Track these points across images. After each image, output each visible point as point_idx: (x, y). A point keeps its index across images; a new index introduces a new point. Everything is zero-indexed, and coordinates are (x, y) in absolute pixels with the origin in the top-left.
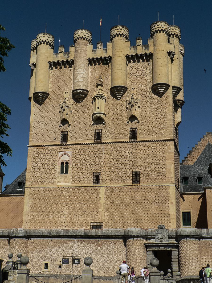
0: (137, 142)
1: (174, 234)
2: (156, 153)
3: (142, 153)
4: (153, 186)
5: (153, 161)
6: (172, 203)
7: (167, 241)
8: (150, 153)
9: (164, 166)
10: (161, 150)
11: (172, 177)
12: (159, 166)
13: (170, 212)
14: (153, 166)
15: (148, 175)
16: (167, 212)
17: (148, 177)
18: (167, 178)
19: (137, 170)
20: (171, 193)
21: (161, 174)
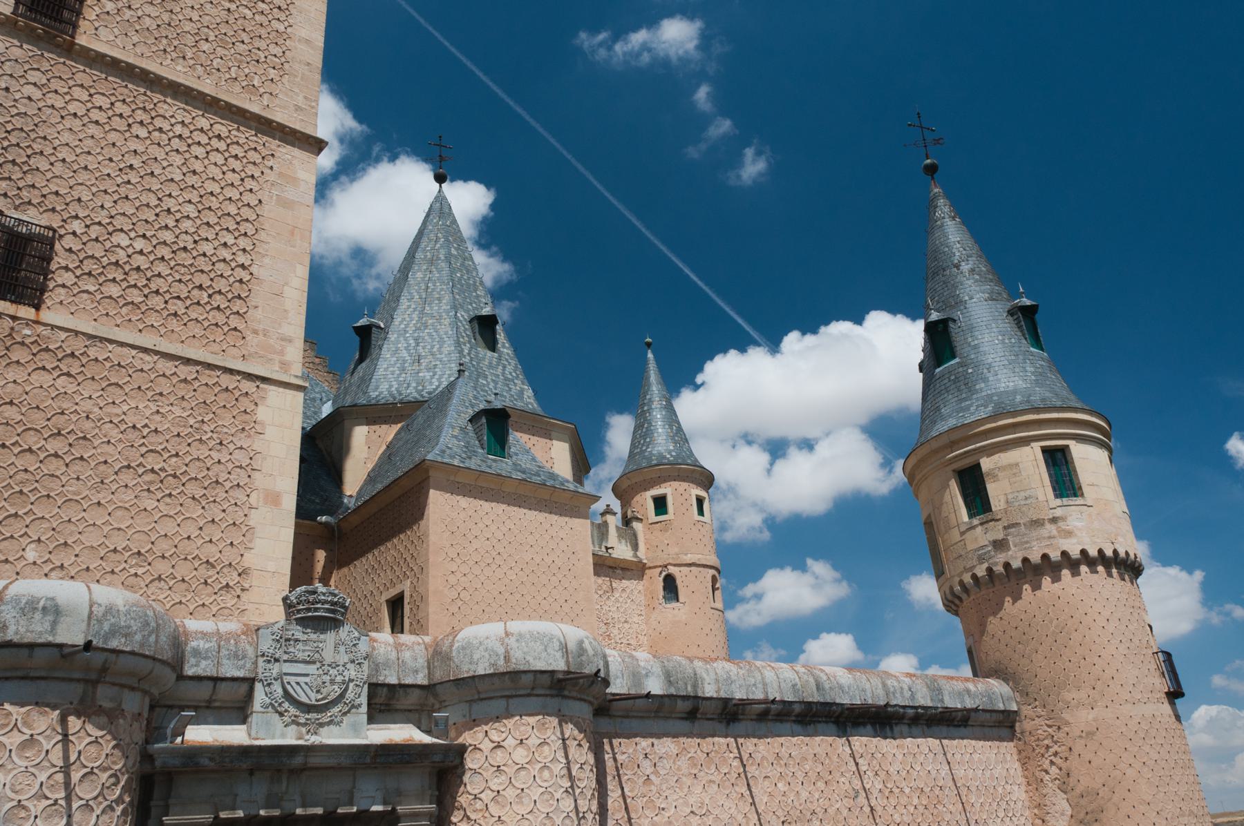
0: (70, 50)
1: (417, 671)
2: (198, 166)
3: (93, 130)
4: (147, 358)
5: (169, 203)
6: (274, 499)
7: (355, 729)
8: (155, 151)
9: (241, 259)
10: (236, 165)
11: (290, 341)
12: (207, 248)
13: (250, 560)
14: (168, 236)
15: (119, 277)
16: (230, 555)
17: (114, 290)
18: (255, 332)
19: (35, 219)
20: (270, 432)
21: (218, 300)
